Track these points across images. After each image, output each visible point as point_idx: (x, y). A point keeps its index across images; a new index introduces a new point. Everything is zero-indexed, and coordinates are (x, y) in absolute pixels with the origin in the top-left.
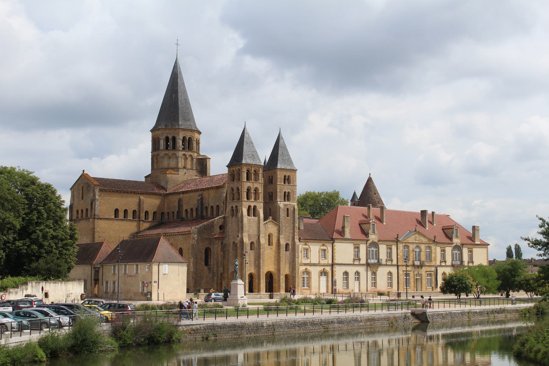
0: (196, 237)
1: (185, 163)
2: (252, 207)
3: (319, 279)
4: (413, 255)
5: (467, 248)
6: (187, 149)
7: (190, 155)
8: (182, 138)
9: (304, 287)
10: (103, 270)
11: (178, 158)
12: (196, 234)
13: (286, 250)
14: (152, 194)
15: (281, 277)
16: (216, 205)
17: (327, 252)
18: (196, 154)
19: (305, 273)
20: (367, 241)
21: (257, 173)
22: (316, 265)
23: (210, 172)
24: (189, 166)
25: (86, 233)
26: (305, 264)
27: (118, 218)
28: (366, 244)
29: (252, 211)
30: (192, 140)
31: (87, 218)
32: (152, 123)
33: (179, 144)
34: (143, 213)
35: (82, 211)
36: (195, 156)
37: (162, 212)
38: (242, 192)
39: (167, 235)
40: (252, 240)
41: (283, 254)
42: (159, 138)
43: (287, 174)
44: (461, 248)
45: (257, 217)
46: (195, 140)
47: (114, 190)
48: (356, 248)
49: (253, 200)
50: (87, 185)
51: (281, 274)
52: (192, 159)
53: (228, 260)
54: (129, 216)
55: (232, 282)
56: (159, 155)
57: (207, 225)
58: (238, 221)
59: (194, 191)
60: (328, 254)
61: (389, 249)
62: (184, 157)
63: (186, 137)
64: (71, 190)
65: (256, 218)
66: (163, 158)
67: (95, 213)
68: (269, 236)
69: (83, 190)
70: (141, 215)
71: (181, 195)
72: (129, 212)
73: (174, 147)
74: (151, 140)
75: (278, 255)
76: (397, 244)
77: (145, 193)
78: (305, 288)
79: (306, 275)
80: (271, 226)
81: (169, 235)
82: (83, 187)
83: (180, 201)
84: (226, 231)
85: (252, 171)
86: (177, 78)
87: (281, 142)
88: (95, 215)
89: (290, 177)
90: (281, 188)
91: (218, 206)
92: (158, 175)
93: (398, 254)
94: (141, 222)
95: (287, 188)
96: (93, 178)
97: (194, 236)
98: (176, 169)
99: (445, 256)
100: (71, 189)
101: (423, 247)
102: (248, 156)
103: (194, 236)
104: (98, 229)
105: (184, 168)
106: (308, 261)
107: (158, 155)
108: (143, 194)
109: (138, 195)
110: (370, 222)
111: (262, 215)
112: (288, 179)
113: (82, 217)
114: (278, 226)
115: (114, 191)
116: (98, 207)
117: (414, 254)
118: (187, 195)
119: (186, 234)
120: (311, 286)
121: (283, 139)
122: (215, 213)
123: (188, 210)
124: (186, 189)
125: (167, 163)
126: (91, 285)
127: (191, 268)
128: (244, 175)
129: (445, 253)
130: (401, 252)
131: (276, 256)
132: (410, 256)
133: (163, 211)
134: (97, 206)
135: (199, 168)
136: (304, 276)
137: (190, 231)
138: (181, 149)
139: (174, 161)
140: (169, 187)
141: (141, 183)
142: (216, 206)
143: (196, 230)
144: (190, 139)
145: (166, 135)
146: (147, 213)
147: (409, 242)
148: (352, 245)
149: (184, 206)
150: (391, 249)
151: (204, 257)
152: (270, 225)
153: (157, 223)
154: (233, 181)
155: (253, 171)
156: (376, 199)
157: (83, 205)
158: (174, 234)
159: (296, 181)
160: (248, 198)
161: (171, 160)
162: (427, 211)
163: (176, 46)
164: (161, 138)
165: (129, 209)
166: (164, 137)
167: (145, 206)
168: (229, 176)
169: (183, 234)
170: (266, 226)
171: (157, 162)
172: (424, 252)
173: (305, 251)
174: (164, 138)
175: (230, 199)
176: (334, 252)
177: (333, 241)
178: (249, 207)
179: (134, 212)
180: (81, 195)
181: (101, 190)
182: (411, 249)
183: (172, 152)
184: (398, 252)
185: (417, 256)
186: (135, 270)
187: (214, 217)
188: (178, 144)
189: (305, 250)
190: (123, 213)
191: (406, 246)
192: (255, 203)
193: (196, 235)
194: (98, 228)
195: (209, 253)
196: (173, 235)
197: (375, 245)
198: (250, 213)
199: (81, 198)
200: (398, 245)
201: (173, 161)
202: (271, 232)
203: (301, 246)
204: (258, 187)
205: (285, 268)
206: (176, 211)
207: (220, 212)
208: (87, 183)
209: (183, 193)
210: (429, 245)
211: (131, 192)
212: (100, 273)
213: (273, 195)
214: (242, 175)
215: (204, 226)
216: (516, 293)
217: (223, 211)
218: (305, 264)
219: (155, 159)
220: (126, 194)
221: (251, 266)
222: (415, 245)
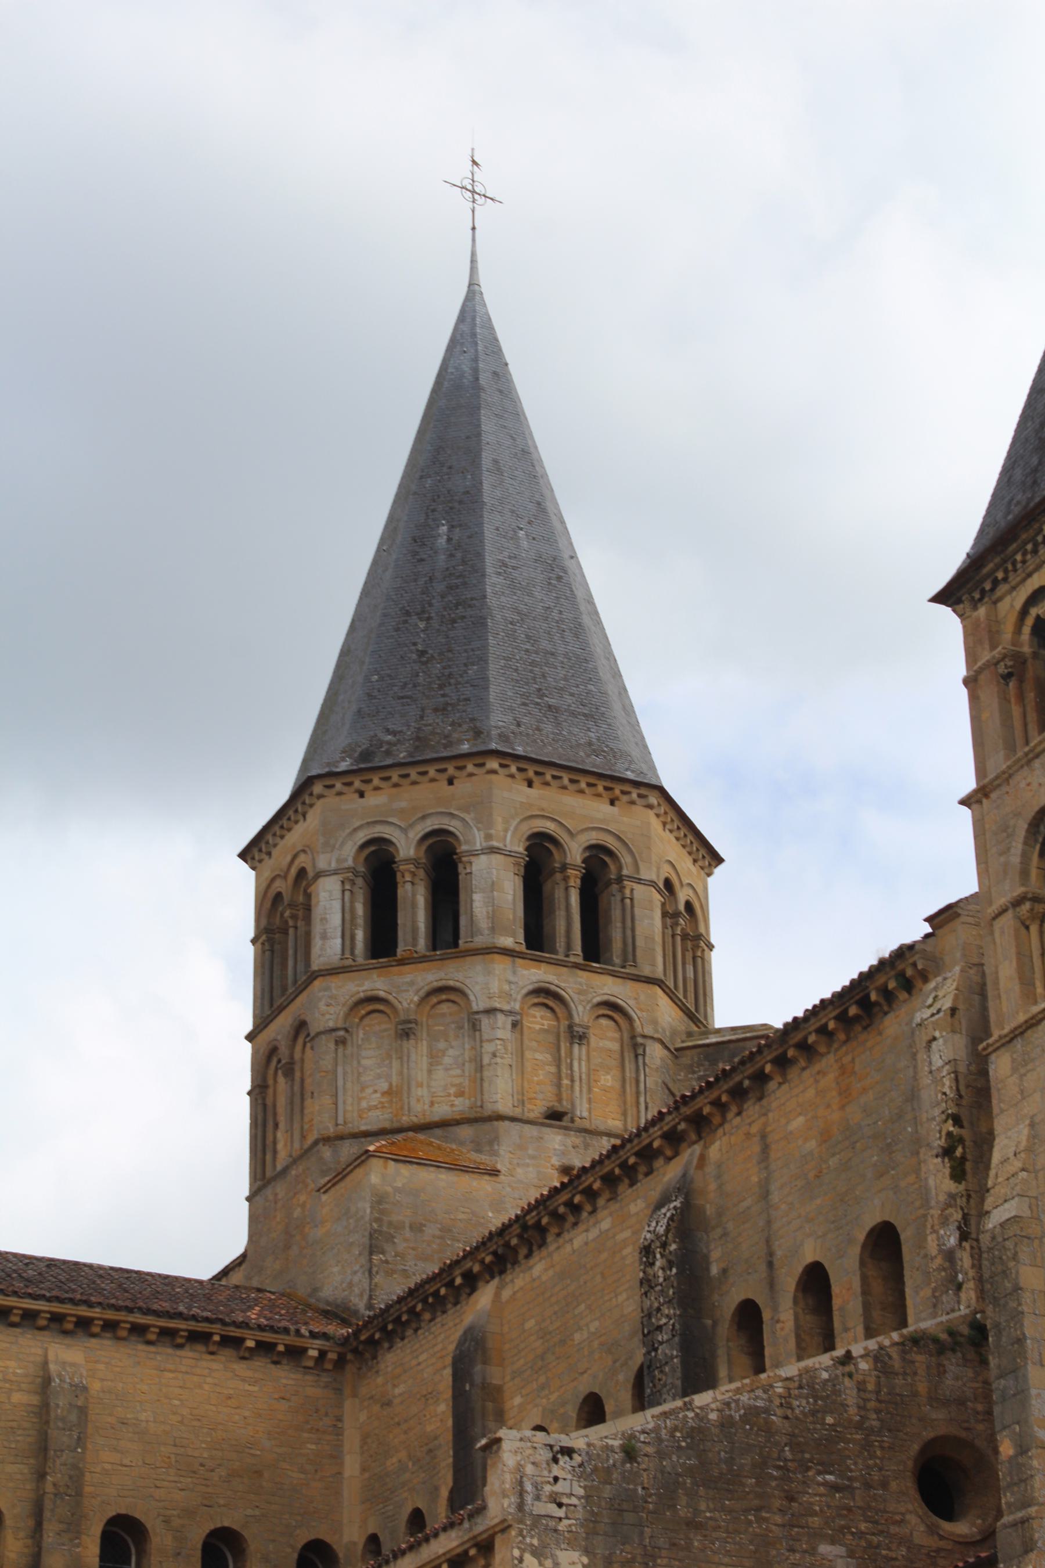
6: (569, 947)
8: (521, 849)
11: (485, 1022)
12: (572, 1544)
16: (861, 1236)
30: (620, 879)
34: (73, 1528)
36: (655, 1022)
37: (304, 1536)
57: (726, 1424)
62: (538, 1020)
66: (341, 1042)
71: (484, 1298)
74: (249, 930)
84: (1022, 1450)
86: (474, 410)
92: (297, 1213)
98: (465, 1132)
105: (555, 1116)
107: (301, 1026)
108: (84, 1325)
125: (385, 1086)
133: (328, 1539)
138: (513, 939)
139: (447, 1060)
142: (856, 1251)
143: (572, 1488)
145: (362, 837)
149: (517, 1400)
161: (419, 1052)
163: (462, 202)
164: (323, 862)
168: (990, 695)
171: (299, 1098)
174: (350, 863)
183: (429, 976)
188: (477, 897)
201: (435, 1058)
207: (916, 1296)
217: (950, 1256)
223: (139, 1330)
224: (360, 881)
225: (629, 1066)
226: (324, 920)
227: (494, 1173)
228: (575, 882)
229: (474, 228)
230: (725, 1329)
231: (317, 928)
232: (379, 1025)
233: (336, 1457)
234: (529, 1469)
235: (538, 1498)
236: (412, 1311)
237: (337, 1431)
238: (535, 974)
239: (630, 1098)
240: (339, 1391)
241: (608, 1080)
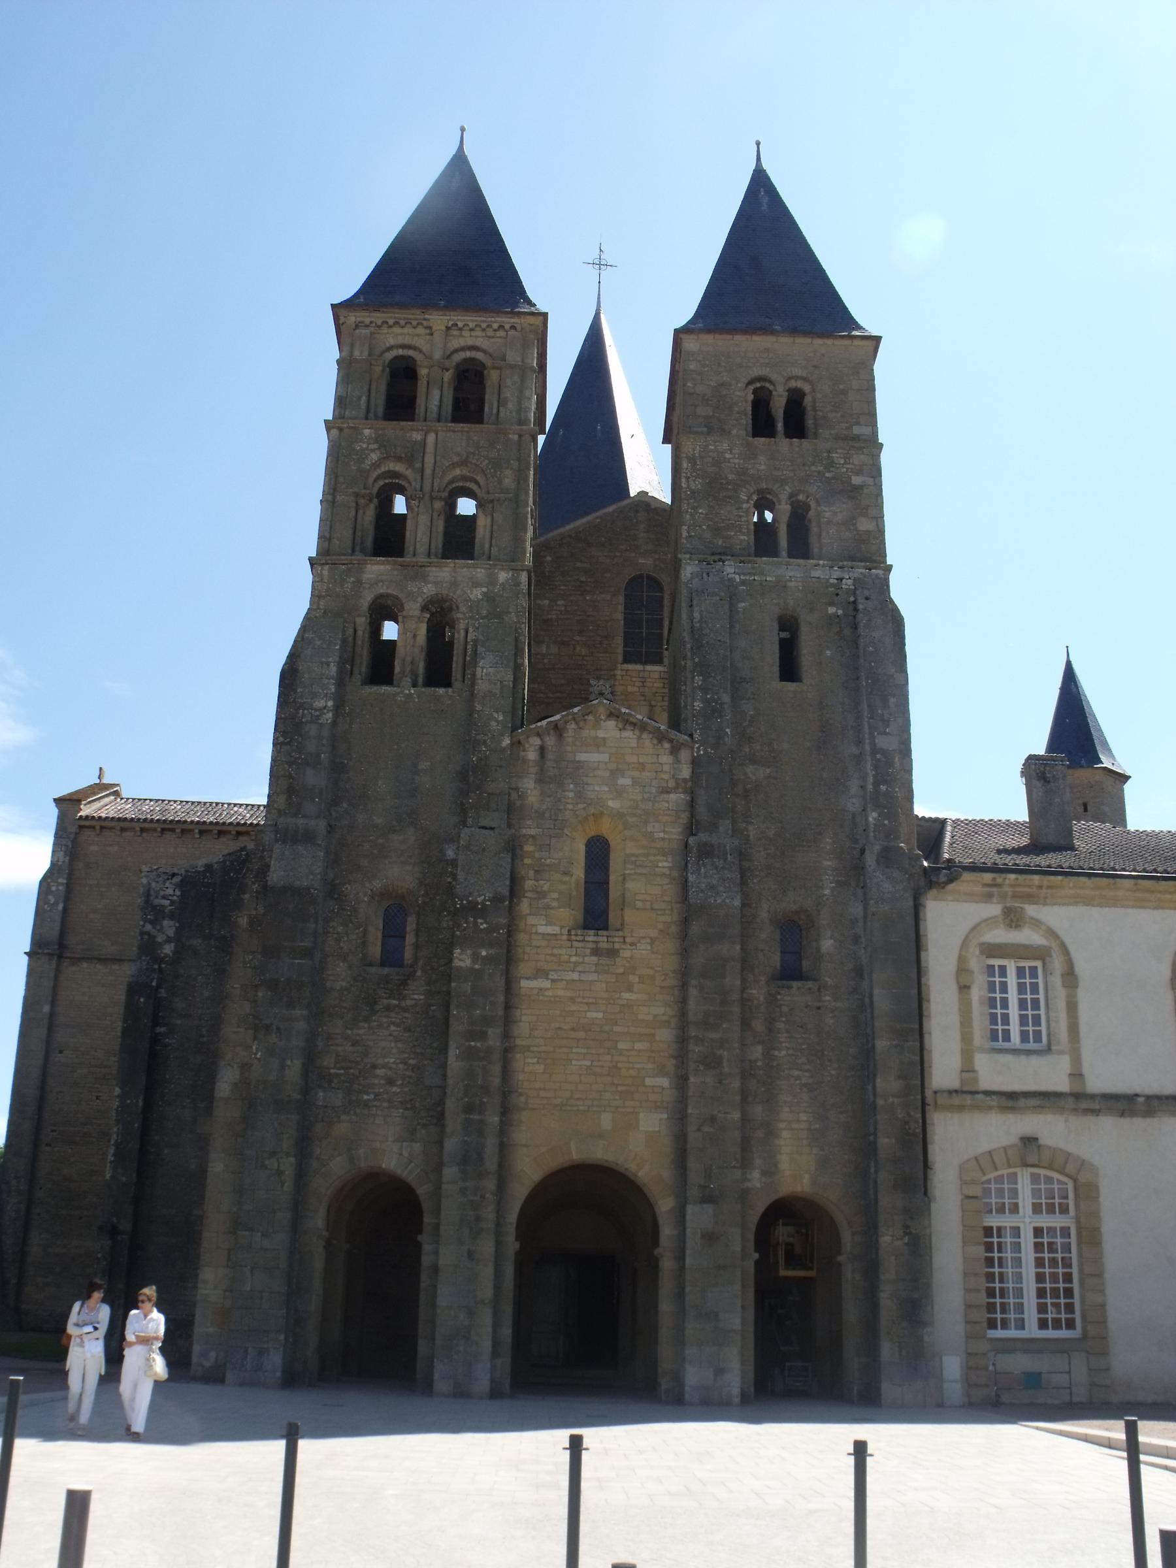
0: (169, 940)
12: (172, 916)
26: (1011, 1100)
78: (1032, 1330)
80: (604, 757)
89: (813, 391)
97: (148, 927)
103: (148, 927)
115: (155, 830)
116: (56, 904)
134: (52, 899)
152: (598, 744)
170: (550, 756)
193: (169, 927)
218: (1011, 1100)
221: (366, 1105)
229: (599, 282)
234: (154, 885)
235: (157, 897)
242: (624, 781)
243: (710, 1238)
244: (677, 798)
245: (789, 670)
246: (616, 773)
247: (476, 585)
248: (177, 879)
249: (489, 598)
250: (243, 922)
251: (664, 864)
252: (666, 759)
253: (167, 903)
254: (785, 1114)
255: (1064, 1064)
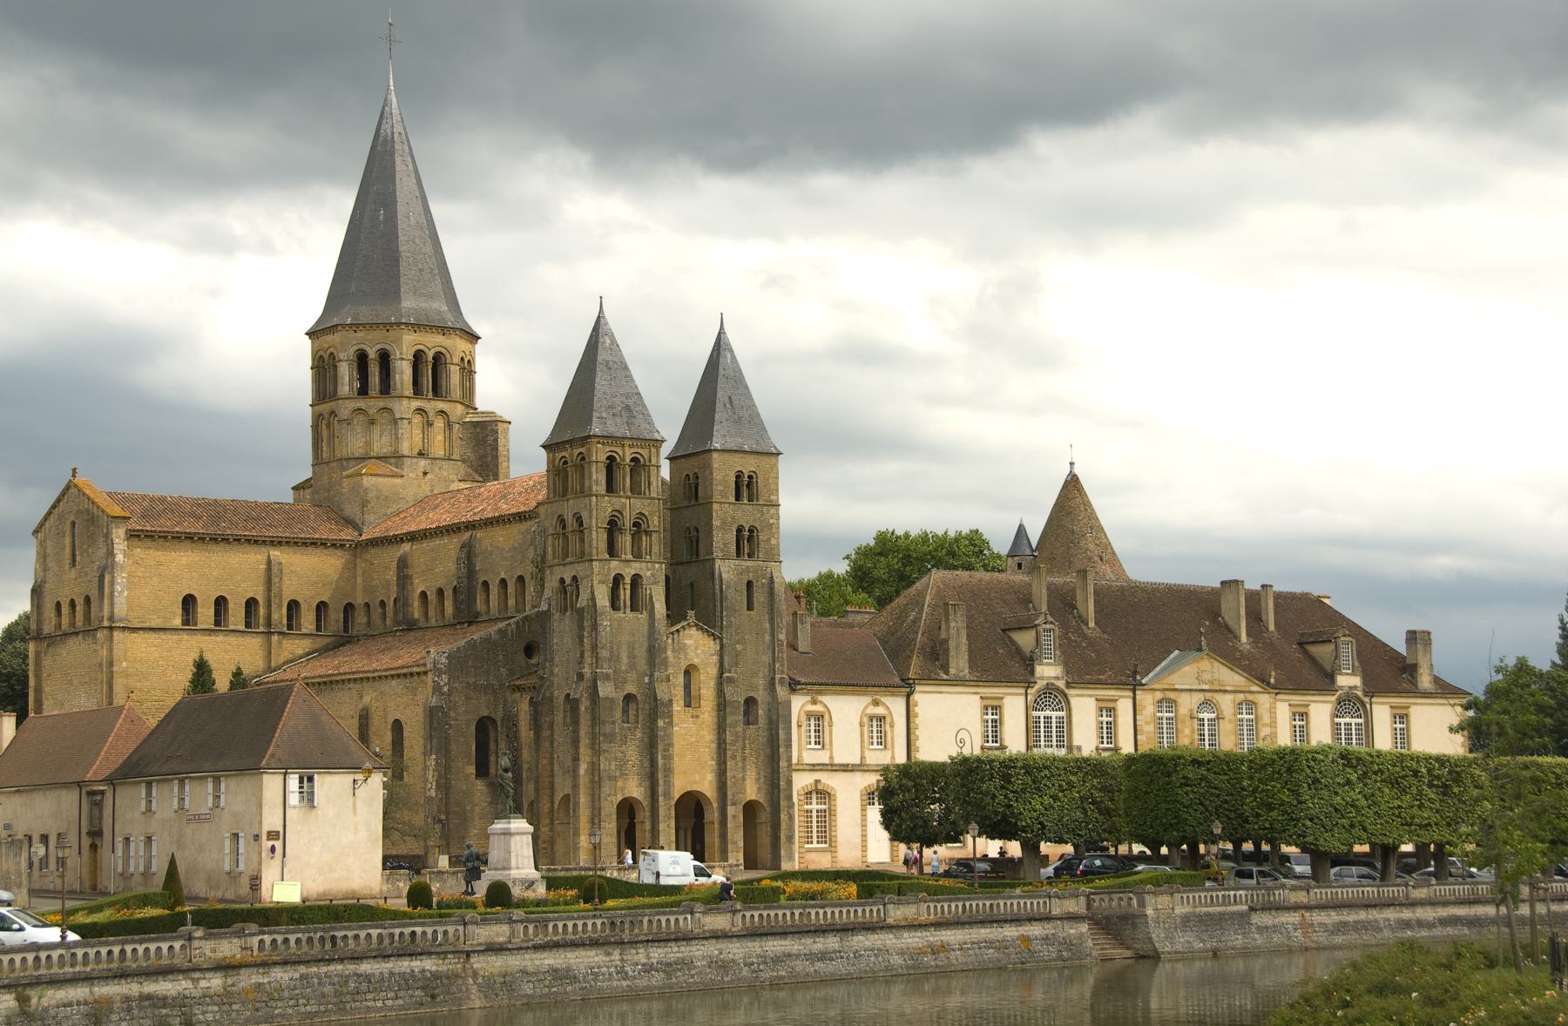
0: (445, 684)
1: (423, 438)
2: (628, 580)
3: (864, 816)
4: (1193, 731)
5: (1388, 706)
7: (443, 412)
9: (812, 843)
10: (117, 801)
13: (748, 723)
14: (312, 543)
15: (731, 810)
17: (888, 726)
18: (460, 409)
19: (814, 796)
20: (1029, 684)
21: (644, 465)
22: (852, 771)
23: (508, 467)
24: (439, 451)
25: (87, 680)
26: (814, 768)
27: (196, 625)
28: (1023, 698)
29: (628, 592)
31: (89, 631)
32: (313, 309)
33: (402, 380)
34: (280, 606)
35: (73, 604)
38: (590, 528)
39: (355, 680)
40: (631, 688)
41: (737, 736)
42: (334, 358)
43: (748, 465)
44: (1364, 705)
45: (644, 612)
46: (456, 360)
47: (177, 532)
48: (990, 711)
49: (630, 557)
50: (86, 518)
51: (729, 802)
52: (449, 425)
53: (552, 758)
54: (232, 619)
55: (493, 826)
56: (336, 416)
58: (581, 628)
59: (448, 530)
60: (892, 732)
61: (1104, 713)
62: (417, 419)
63: (426, 350)
64: (37, 537)
65: (643, 616)
67: (112, 611)
68: (687, 673)
69: (74, 537)
70: (275, 616)
71: (406, 547)
72: (231, 605)
73: (386, 388)
74: (310, 363)
75: (719, 739)
76: (1135, 694)
77: (287, 542)
78: (815, 845)
79: (817, 804)
81: (362, 679)
82: (73, 524)
83: (403, 563)
85: (624, 460)
87: (726, 360)
88: (111, 619)
90: (725, 514)
91: (521, 579)
93: (1138, 728)
94: (275, 638)
95: (746, 515)
96: (109, 494)
98: (393, 460)
99: (1308, 735)
100: (36, 532)
101: (1226, 702)
102: (612, 412)
104: (124, 664)
105: (421, 454)
106: (822, 757)
107: (333, 413)
108: (280, 543)
109: (263, 549)
110: (1036, 622)
111: (660, 608)
112: (749, 485)
113: (73, 624)
114: (718, 641)
116: (122, 591)
117: (1196, 727)
118: (425, 545)
119: (412, 674)
120: (833, 839)
121: (731, 351)
122: (511, 602)
123: (428, 593)
124: (423, 526)
126: (80, 853)
127: (429, 786)
128: (598, 477)
129: (1307, 723)
130: (1147, 723)
131: (713, 742)
132: (1180, 735)
134: (118, 588)
135: (472, 456)
136: (809, 807)
137: (425, 665)
138: (409, 391)
140: (370, 518)
141: (279, 508)
144: (438, 358)
145: (356, 348)
146: (293, 606)
147: (1177, 687)
148: (977, 697)
150: (1111, 711)
151: (474, 748)
152: (691, 637)
153: (329, 640)
154: (564, 495)
155: (628, 460)
156: (1092, 546)
157: (69, 587)
158: (376, 674)
159: (777, 490)
160: (612, 550)
161: (376, 430)
162: (1243, 582)
164: (342, 356)
165: (232, 594)
166: (352, 351)
167: (286, 583)
169: (405, 675)
171: (332, 437)
172: (1230, 721)
173: (812, 722)
175: (554, 553)
176: (912, 725)
177: (908, 690)
178: (618, 579)
179: (251, 604)
180: (68, 550)
181: (133, 535)
182: (1183, 710)
183: (381, 404)
184: (1138, 723)
185: (1207, 737)
186: (210, 798)
187: (509, 615)
189: (812, 720)
190: (212, 610)
191: (1167, 703)
192: (637, 565)
194: (126, 660)
195: (492, 735)
196: (374, 678)
197: (1053, 696)
198: (619, 600)
199: (68, 561)
200: (1138, 697)
202: (696, 661)
203: (799, 704)
204: (647, 514)
205: (744, 779)
206: (392, 599)
208: (88, 510)
209: (412, 537)
210: (1250, 697)
211: (239, 540)
212: (107, 812)
213: (702, 536)
214: (590, 473)
215: (472, 645)
216: (878, 817)
218: (814, 768)
219: (324, 426)
220: (221, 544)
222: (1200, 697)
223: (296, 543)
224: (355, 364)
225: (447, 432)
226: (342, 378)
227: (403, 476)
228: (430, 367)
230: (479, 586)
231: (339, 381)
232: (361, 418)
233: (355, 577)
236: (382, 542)
237: (355, 568)
238: (416, 404)
239: (447, 444)
240: (355, 556)
241: (440, 438)
242: (699, 651)
243: (734, 817)
244: (715, 658)
245: (750, 607)
246: (696, 648)
247: (648, 570)
248: (446, 655)
249: (653, 575)
250: (583, 708)
251: (712, 683)
252: (712, 642)
253: (442, 666)
254: (748, 773)
255: (828, 754)
